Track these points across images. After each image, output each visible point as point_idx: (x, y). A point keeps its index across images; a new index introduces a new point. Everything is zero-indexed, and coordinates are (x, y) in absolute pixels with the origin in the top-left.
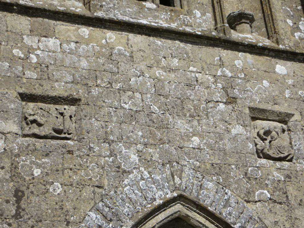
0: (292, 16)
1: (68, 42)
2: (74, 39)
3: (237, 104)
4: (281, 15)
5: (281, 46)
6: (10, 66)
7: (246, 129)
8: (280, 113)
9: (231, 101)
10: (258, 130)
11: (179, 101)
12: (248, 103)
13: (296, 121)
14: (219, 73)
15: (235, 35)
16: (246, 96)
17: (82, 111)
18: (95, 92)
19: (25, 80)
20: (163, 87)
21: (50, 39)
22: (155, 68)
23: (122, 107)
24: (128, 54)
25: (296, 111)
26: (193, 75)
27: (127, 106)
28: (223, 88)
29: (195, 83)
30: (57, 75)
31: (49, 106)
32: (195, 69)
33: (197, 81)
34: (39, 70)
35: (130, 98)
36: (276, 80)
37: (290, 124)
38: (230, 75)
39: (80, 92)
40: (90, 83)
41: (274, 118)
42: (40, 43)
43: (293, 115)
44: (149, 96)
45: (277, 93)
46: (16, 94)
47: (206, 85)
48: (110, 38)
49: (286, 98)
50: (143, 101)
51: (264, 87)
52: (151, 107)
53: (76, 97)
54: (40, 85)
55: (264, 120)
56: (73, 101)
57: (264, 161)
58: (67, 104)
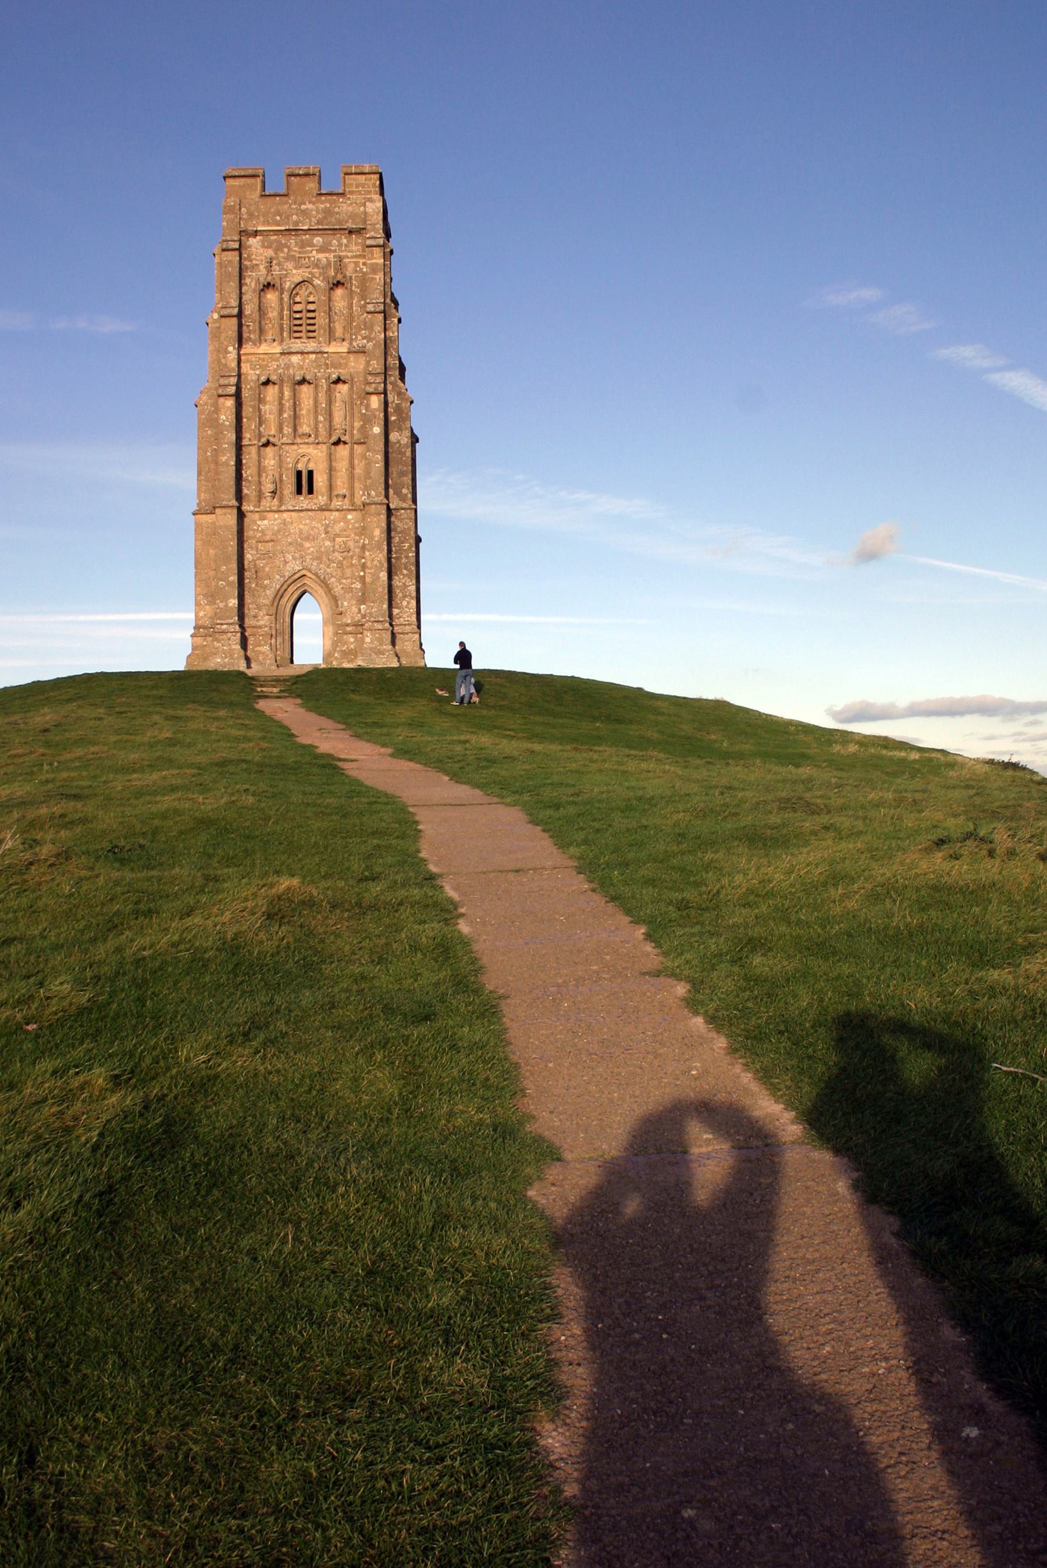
9: (327, 533)
39: (274, 537)
57: (336, 554)
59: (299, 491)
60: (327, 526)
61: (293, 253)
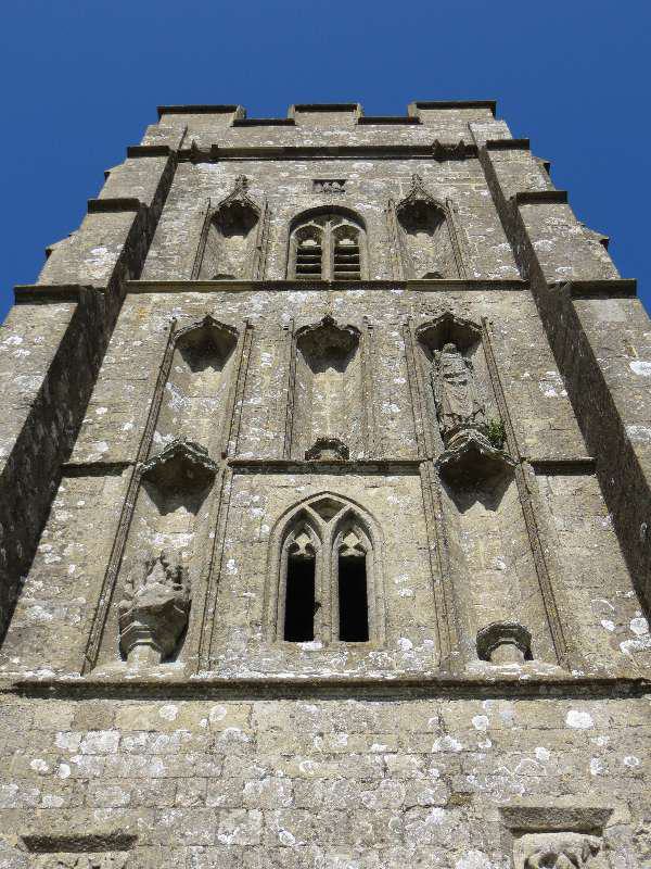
0: (615, 612)
1: (135, 733)
2: (148, 726)
3: (473, 806)
4: (587, 614)
5: (574, 673)
6: (18, 791)
7: (491, 858)
8: (578, 811)
9: (459, 799)
10: (523, 857)
11: (342, 815)
12: (498, 800)
13: (619, 823)
14: (436, 747)
15: (476, 669)
16: (493, 785)
17: (136, 859)
18: (168, 819)
19: (39, 813)
20: (311, 790)
21: (103, 732)
22: (299, 758)
23: (217, 843)
24: (246, 740)
25: (616, 800)
26: (378, 759)
27: (228, 840)
28: (442, 776)
29: (382, 774)
30: (102, 795)
31: (74, 856)
32: (383, 748)
33: (385, 770)
34: (69, 790)
35: (238, 822)
36: (580, 744)
37: (607, 832)
38: (459, 747)
39: (141, 823)
40: (162, 803)
41: (566, 825)
42: (84, 742)
43: (611, 812)
44: (278, 813)
45: (568, 769)
46: (15, 840)
47: (405, 773)
48: (216, 715)
49: (590, 776)
50: (265, 825)
51: (538, 760)
52: (281, 835)
53: (130, 833)
54: (65, 818)
55: (544, 831)
56: (123, 841)
58: (112, 849)
59: (298, 625)
60: (458, 764)
61: (299, 177)
